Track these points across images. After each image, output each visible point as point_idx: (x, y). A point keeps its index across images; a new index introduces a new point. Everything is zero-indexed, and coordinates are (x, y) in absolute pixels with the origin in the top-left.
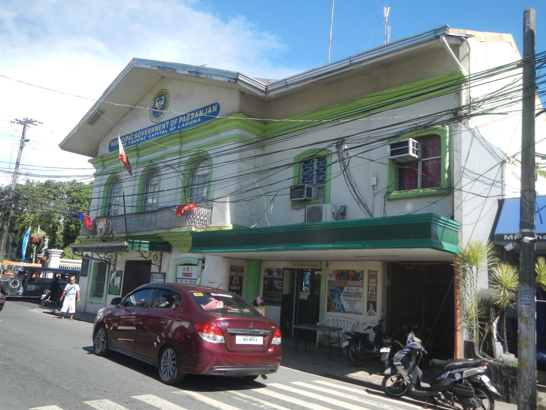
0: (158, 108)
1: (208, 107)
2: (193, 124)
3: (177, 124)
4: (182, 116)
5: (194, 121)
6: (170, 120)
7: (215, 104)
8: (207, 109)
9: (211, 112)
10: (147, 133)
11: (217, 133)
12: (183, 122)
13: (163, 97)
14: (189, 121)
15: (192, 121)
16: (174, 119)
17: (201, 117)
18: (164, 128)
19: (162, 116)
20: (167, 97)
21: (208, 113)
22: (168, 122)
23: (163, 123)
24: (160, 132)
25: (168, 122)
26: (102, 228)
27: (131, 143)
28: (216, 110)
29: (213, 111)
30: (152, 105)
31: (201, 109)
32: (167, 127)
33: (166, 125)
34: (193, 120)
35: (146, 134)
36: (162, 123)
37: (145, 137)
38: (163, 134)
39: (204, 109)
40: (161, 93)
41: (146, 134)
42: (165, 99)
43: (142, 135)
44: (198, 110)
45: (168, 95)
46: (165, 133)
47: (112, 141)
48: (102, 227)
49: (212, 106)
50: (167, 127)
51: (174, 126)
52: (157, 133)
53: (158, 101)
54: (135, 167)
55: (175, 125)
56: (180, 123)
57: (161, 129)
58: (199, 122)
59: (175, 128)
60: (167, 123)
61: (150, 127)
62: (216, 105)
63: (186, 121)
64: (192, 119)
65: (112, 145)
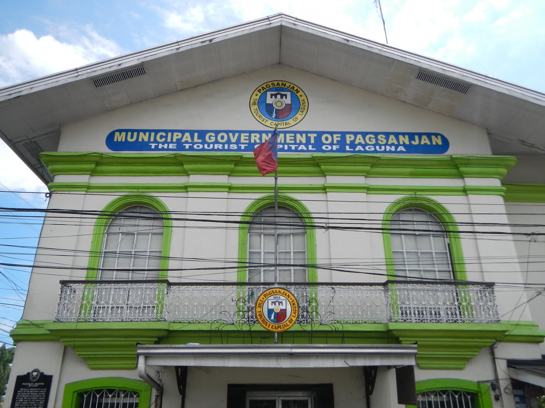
0: (277, 106)
1: (420, 135)
2: (385, 151)
3: (342, 143)
4: (355, 134)
5: (388, 148)
6: (320, 134)
7: (436, 135)
8: (417, 137)
9: (429, 143)
10: (250, 139)
11: (461, 176)
12: (357, 142)
13: (289, 94)
14: (375, 145)
15: (383, 148)
16: (332, 133)
17: (404, 145)
18: (304, 140)
19: (291, 122)
20: (298, 94)
21: (422, 143)
22: (315, 135)
23: (301, 133)
24: (293, 147)
25: (315, 135)
26: (284, 312)
27: (195, 147)
28: (440, 142)
29: (434, 143)
30: (256, 97)
31: (404, 134)
32: (312, 141)
33: (308, 139)
34: (385, 145)
35: (247, 141)
36: (295, 133)
37: (243, 147)
38: (302, 151)
39: (411, 136)
40: (278, 84)
41: (242, 141)
42: (295, 97)
43: (234, 140)
44: (397, 135)
45: (301, 93)
46: (308, 151)
47: (120, 131)
48: (283, 307)
49: (429, 135)
50: (312, 141)
51: (332, 144)
52: (281, 146)
53: (276, 96)
54: (84, 193)
55: (335, 142)
56: (348, 142)
57: (293, 142)
58: (401, 152)
59: (335, 148)
60: (312, 136)
61: (260, 132)
62: (439, 137)
63: (367, 144)
64: (379, 142)
65: (119, 138)
